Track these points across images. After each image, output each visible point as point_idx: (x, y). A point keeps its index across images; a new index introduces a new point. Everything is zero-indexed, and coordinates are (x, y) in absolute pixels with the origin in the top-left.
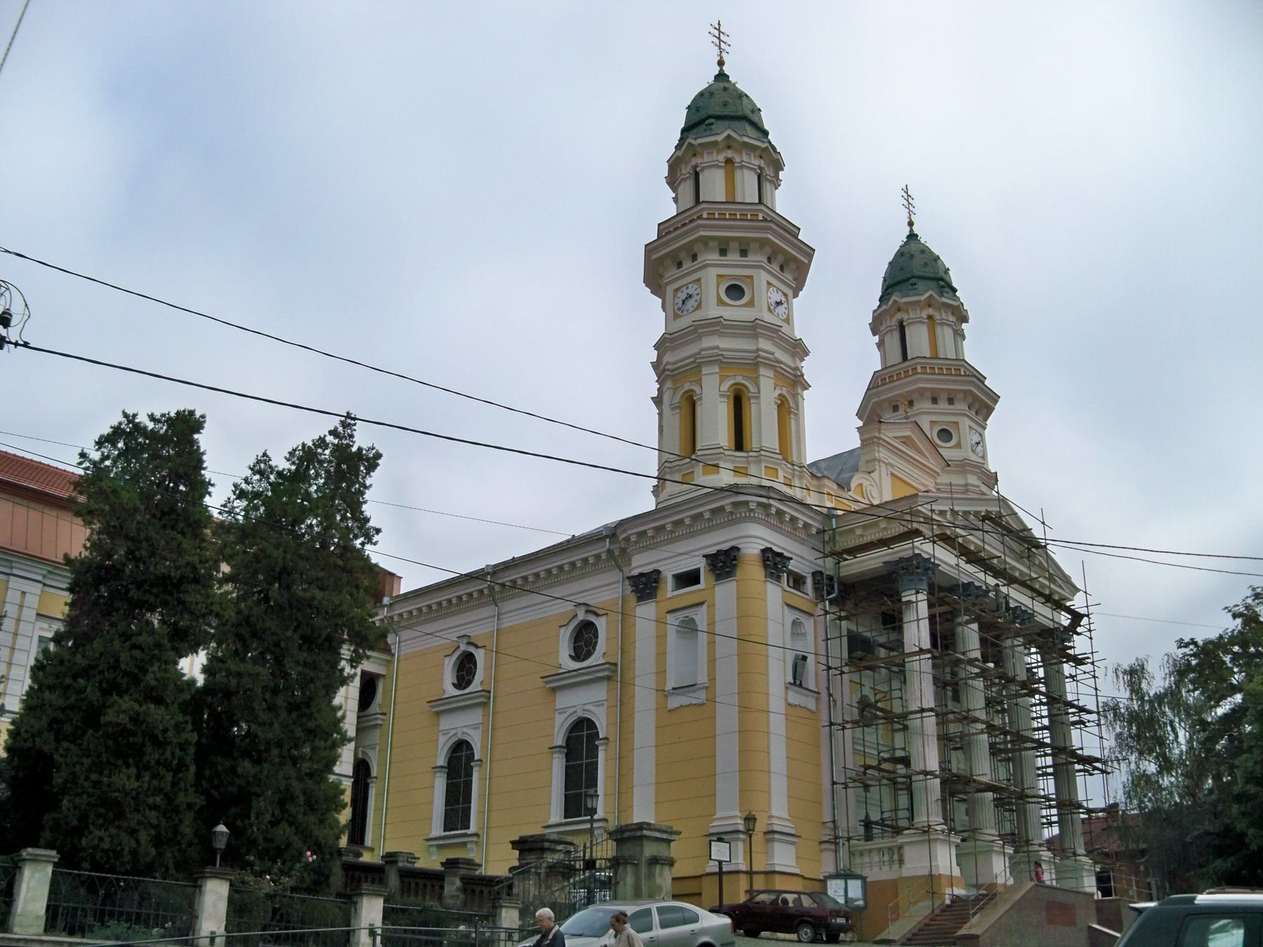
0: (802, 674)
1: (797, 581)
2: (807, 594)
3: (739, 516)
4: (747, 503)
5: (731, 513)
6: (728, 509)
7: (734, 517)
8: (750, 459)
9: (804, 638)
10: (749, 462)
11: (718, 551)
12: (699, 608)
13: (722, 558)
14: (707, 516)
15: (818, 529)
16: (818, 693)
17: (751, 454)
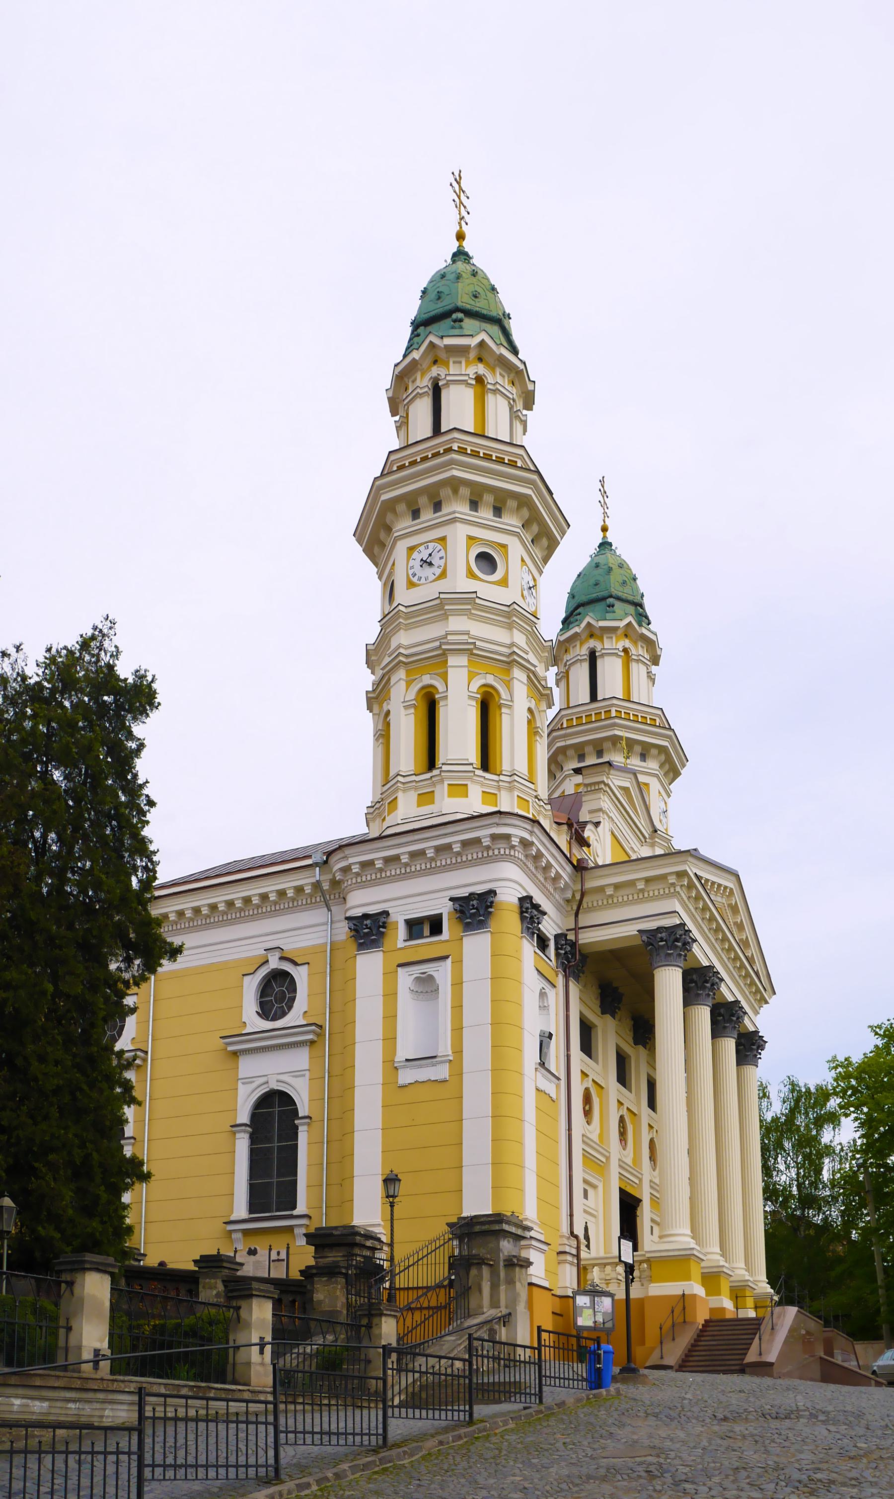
0: (546, 1053)
1: (542, 943)
2: (551, 961)
3: (496, 852)
4: (507, 837)
5: (488, 848)
6: (486, 842)
7: (491, 853)
8: (501, 783)
9: (545, 1012)
10: (499, 788)
11: (470, 894)
12: (441, 963)
13: (475, 902)
14: (457, 848)
15: (566, 882)
16: (558, 1079)
17: (502, 777)
